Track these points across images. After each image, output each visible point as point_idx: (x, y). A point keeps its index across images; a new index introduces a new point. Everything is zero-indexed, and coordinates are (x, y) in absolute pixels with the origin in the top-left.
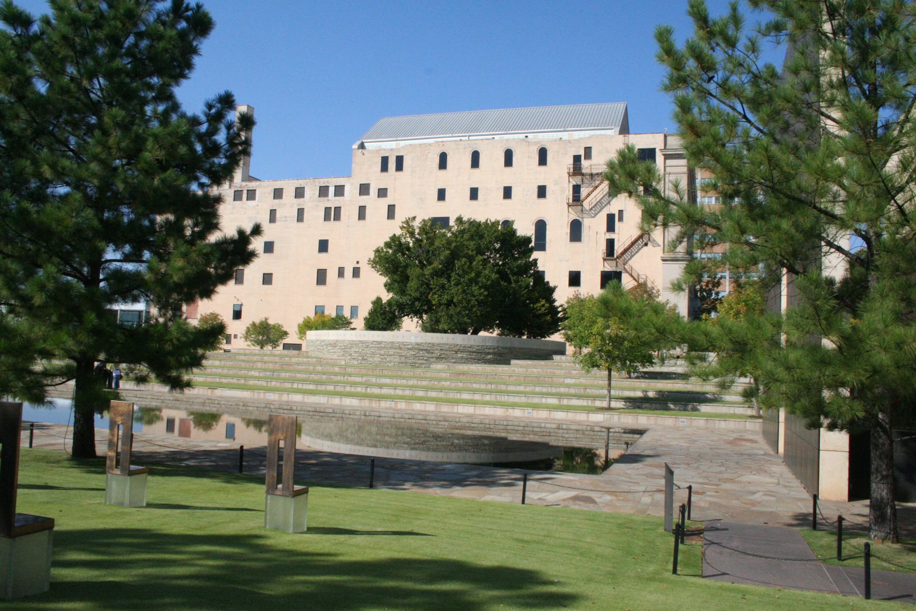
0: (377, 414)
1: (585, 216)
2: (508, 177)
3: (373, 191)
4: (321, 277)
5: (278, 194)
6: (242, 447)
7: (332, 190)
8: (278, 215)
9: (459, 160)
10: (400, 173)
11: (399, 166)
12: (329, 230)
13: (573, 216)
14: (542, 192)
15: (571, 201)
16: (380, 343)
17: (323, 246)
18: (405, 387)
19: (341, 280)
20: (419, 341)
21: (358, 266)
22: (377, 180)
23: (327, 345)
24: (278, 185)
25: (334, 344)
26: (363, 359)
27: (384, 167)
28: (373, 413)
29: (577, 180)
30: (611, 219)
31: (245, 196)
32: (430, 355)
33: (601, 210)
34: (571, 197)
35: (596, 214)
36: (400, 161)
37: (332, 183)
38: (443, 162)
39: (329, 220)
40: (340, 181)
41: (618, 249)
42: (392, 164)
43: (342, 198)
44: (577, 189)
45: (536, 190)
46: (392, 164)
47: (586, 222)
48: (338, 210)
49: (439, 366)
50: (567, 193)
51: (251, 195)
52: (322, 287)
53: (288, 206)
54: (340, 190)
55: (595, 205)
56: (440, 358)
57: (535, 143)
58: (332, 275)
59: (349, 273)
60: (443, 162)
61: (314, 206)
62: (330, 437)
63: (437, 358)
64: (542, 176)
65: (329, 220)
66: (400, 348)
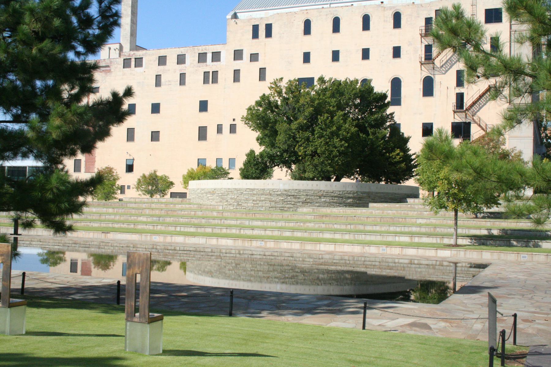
0: (251, 253)
1: (436, 73)
2: (366, 39)
3: (246, 56)
4: (202, 134)
5: (162, 61)
6: (119, 282)
7: (209, 56)
8: (163, 80)
10: (269, 39)
11: (269, 34)
13: (426, 74)
14: (397, 52)
15: (423, 60)
16: (253, 190)
17: (203, 106)
18: (273, 229)
19: (220, 135)
20: (287, 187)
21: (234, 123)
22: (249, 46)
23: (206, 193)
24: (162, 53)
25: (213, 192)
26: (238, 205)
27: (255, 35)
28: (246, 252)
29: (429, 40)
31: (133, 63)
32: (296, 200)
33: (451, 67)
34: (423, 56)
35: (446, 71)
36: (269, 29)
37: (210, 50)
38: (307, 28)
39: (209, 83)
40: (216, 49)
41: (467, 101)
42: (262, 32)
43: (219, 63)
44: (428, 49)
45: (391, 51)
46: (262, 32)
47: (438, 79)
48: (215, 73)
49: (305, 210)
50: (419, 52)
51: (139, 62)
52: (203, 143)
53: (171, 71)
54: (216, 56)
55: (444, 64)
56: (305, 203)
57: (391, 8)
58: (211, 132)
59: (226, 129)
60: (307, 28)
61: (194, 71)
62: (210, 274)
63: (303, 203)
64: (397, 37)
65: (209, 83)
66: (271, 195)
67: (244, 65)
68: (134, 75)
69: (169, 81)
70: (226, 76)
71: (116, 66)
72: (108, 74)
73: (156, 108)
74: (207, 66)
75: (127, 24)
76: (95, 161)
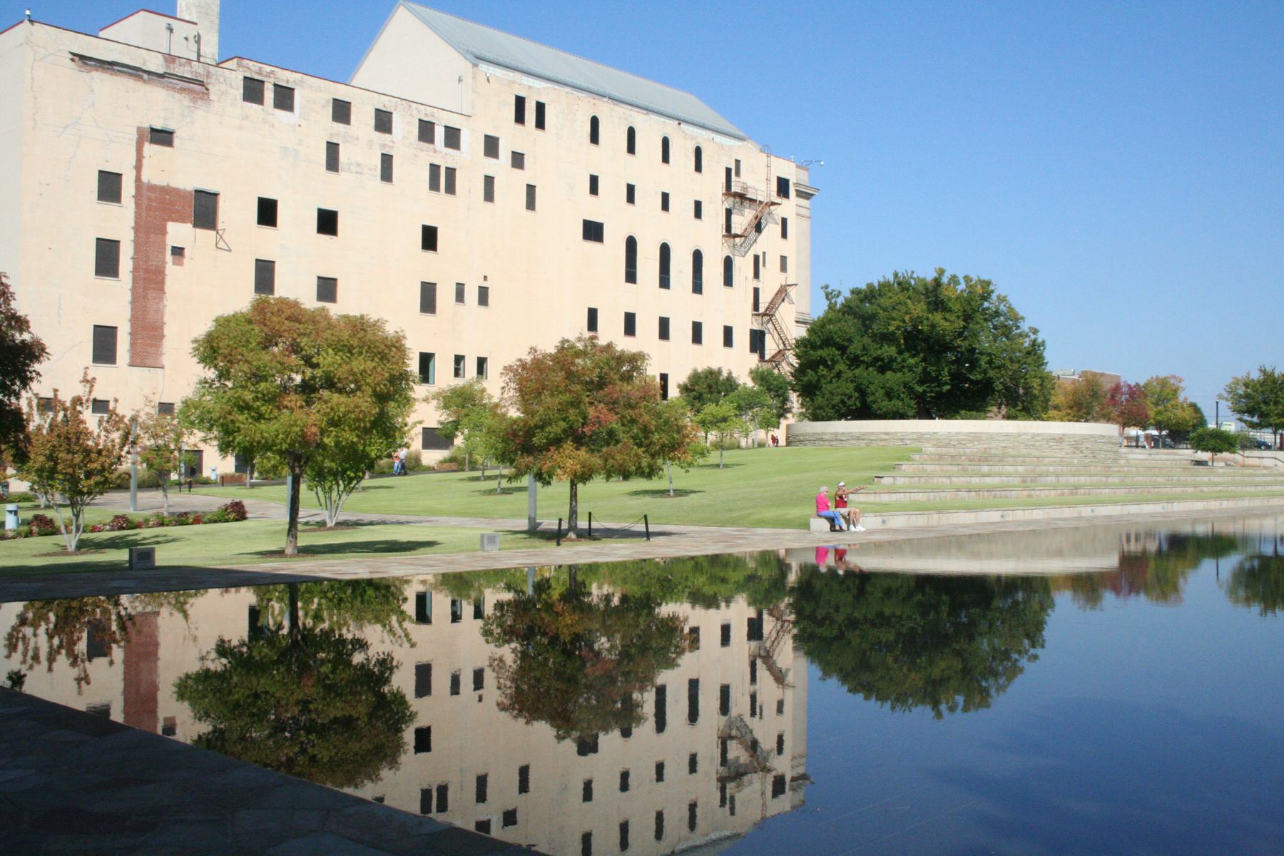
9: (612, 134)
12: (435, 209)
13: (727, 253)
16: (1103, 437)
17: (430, 238)
21: (485, 284)
25: (1060, 439)
27: (520, 118)
29: (729, 203)
30: (756, 258)
31: (269, 95)
44: (729, 213)
51: (284, 98)
54: (453, 137)
58: (444, 296)
59: (471, 295)
67: (500, 167)
68: (273, 126)
69: (359, 165)
70: (470, 184)
71: (223, 87)
72: (200, 102)
73: (327, 222)
74: (435, 151)
76: (163, 336)
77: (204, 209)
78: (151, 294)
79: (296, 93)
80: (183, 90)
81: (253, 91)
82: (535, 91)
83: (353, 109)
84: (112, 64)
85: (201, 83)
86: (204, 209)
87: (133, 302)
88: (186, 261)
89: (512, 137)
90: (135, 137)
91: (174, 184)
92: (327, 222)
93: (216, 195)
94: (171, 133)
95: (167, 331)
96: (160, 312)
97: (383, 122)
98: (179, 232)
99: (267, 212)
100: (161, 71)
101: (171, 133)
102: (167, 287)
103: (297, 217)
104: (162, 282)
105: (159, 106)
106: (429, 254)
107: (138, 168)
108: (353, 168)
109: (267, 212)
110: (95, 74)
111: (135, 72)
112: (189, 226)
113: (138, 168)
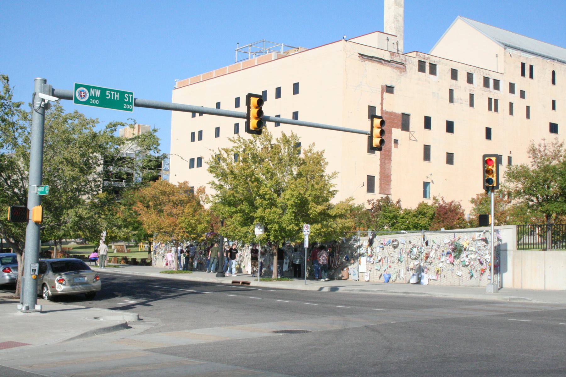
17: (488, 133)
27: (523, 74)
68: (429, 83)
69: (461, 99)
70: (503, 106)
71: (411, 65)
72: (403, 73)
73: (450, 127)
75: (400, 15)
77: (405, 122)
78: (387, 161)
79: (437, 66)
80: (397, 67)
81: (421, 67)
82: (530, 60)
83: (458, 73)
84: (372, 57)
85: (403, 64)
86: (405, 122)
87: (381, 165)
88: (399, 146)
89: (521, 83)
90: (380, 90)
91: (394, 111)
92: (450, 127)
93: (409, 115)
94: (393, 88)
95: (393, 178)
96: (390, 169)
97: (470, 78)
98: (396, 133)
99: (428, 123)
100: (389, 60)
101: (393, 88)
102: (393, 158)
103: (439, 125)
104: (391, 156)
105: (387, 75)
106: (489, 141)
107: (382, 104)
108: (459, 101)
109: (428, 123)
110: (367, 62)
111: (380, 60)
112: (400, 130)
113: (382, 104)
